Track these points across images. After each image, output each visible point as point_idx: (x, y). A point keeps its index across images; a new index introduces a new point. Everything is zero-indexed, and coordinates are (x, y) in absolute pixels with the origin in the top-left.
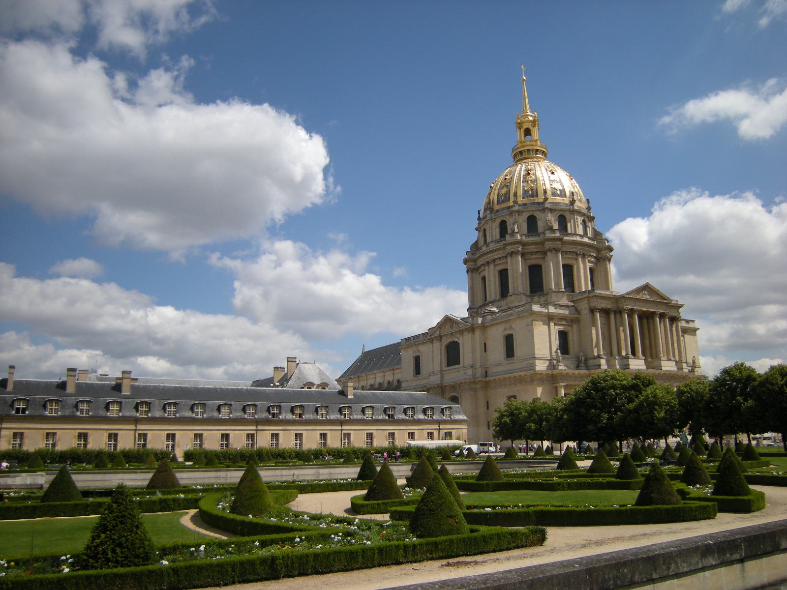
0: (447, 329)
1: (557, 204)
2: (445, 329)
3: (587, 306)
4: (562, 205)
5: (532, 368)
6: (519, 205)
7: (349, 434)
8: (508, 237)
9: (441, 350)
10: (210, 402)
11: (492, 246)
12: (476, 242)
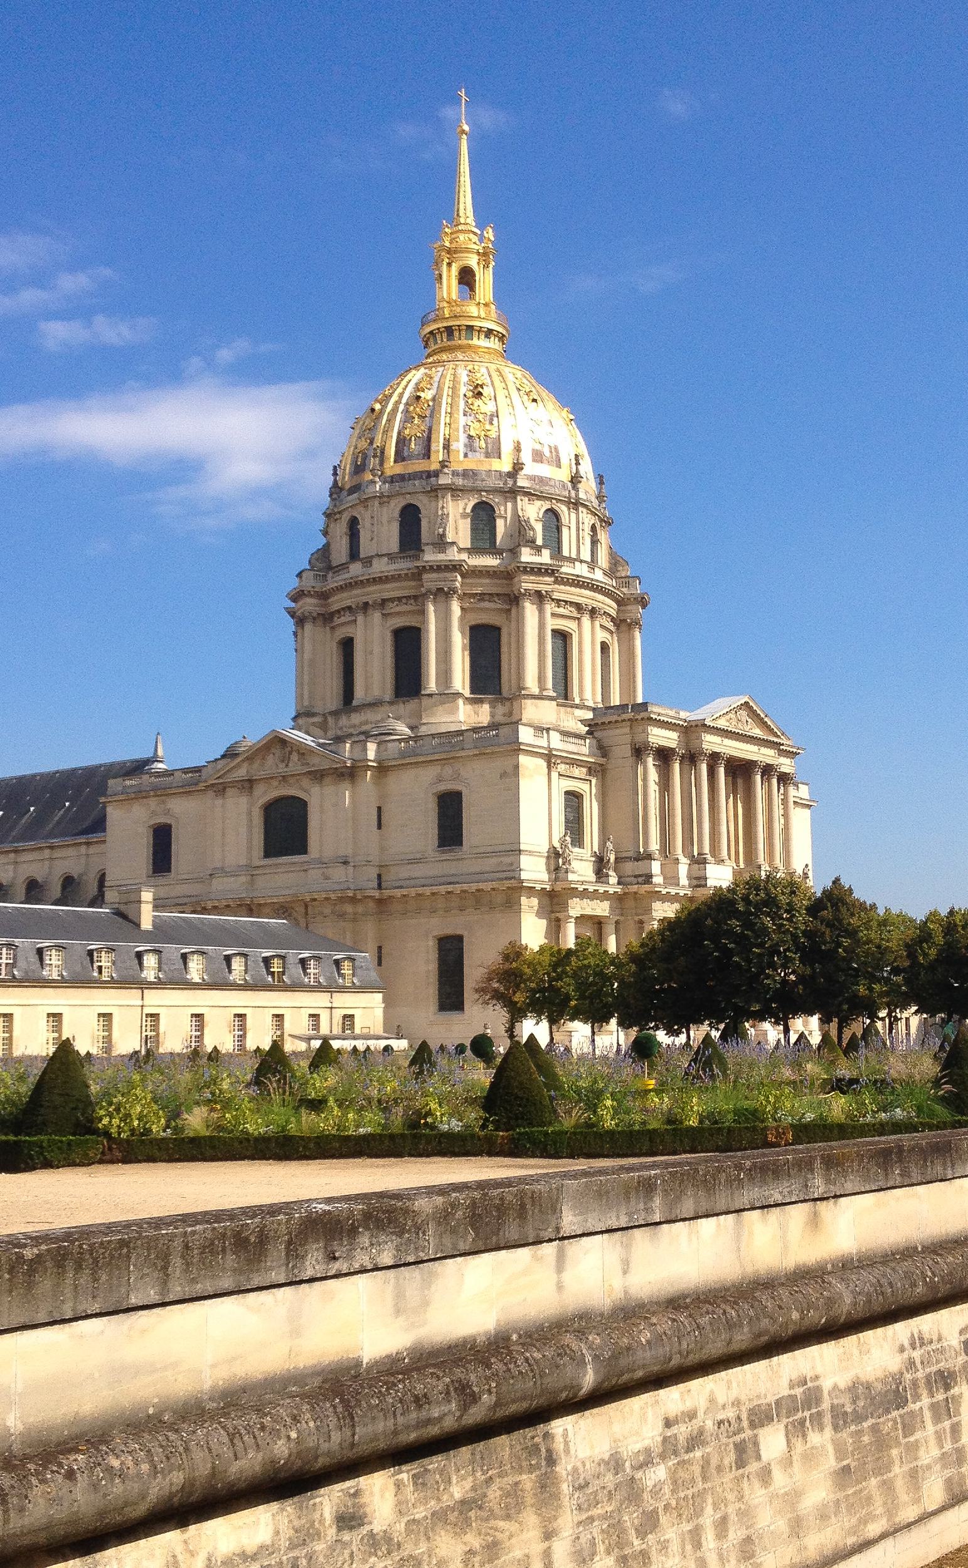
0: (272, 764)
1: (542, 480)
2: (262, 765)
3: (628, 739)
4: (552, 483)
5: (511, 874)
6: (455, 473)
7: (155, 1017)
8: (430, 556)
9: (249, 813)
11: (381, 567)
12: (325, 551)
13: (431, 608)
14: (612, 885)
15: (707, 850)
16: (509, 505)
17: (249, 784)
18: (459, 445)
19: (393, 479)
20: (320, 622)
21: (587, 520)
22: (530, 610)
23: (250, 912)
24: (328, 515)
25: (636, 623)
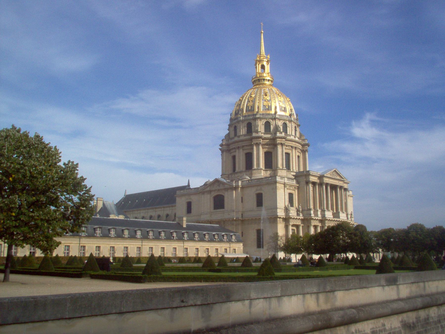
1: (282, 116)
6: (260, 115)
7: (187, 249)
8: (254, 135)
10: (117, 227)
11: (241, 138)
12: (228, 134)
13: (255, 148)
14: (301, 217)
15: (325, 207)
16: (274, 122)
17: (210, 192)
19: (245, 116)
22: (279, 147)
23: (211, 223)
24: (229, 125)
25: (307, 151)
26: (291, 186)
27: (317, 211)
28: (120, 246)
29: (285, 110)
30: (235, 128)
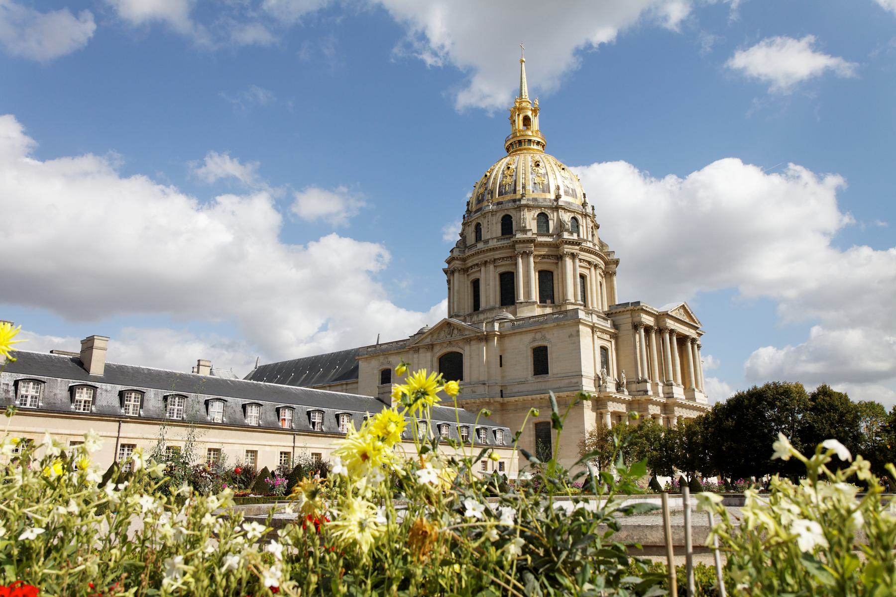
1: (569, 203)
3: (630, 320)
9: (432, 361)
11: (493, 244)
13: (520, 260)
14: (626, 395)
15: (672, 379)
16: (555, 214)
18: (530, 187)
20: (462, 272)
21: (591, 224)
22: (569, 262)
26: (604, 331)
27: (657, 384)
28: (236, 447)
29: (574, 195)
30: (478, 228)
